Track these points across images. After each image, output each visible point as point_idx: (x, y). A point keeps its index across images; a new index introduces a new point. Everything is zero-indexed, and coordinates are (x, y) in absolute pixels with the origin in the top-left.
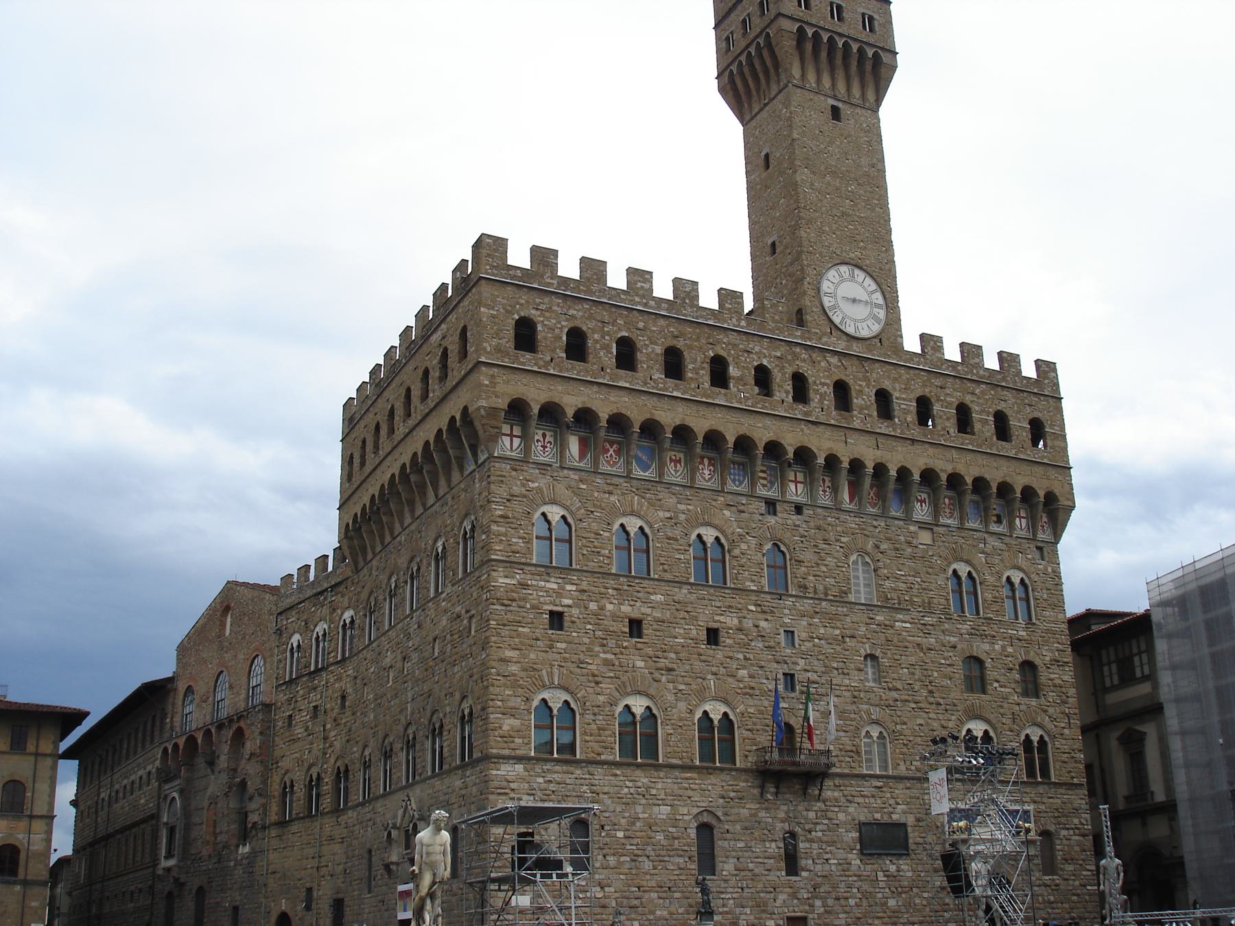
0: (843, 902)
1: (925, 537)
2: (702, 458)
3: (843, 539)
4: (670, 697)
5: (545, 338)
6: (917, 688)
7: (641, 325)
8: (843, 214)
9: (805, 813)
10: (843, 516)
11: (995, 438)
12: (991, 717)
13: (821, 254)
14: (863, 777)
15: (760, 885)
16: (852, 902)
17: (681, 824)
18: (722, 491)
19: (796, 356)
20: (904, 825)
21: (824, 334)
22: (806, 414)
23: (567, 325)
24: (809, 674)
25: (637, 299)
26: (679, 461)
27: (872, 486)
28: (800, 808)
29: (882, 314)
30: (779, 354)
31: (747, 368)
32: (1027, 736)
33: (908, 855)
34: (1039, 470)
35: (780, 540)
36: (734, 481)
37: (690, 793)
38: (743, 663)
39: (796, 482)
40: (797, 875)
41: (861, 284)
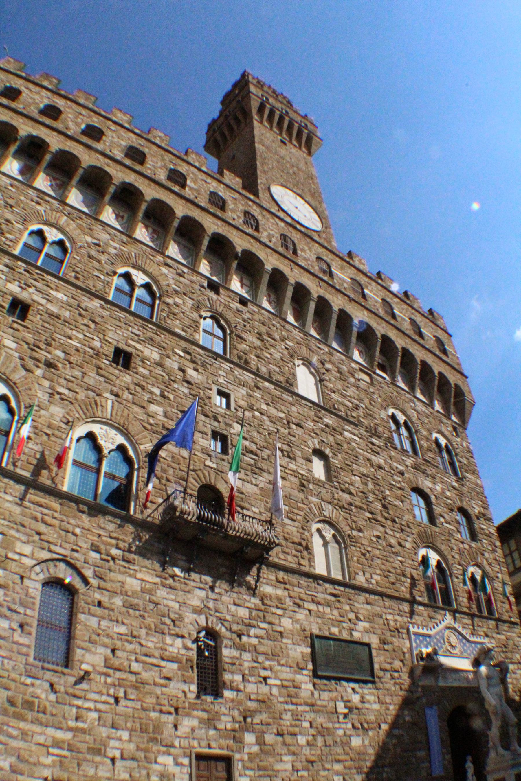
0: (289, 739)
4: (42, 396)
6: (371, 499)
9: (233, 608)
10: (288, 326)
12: (443, 548)
14: (316, 578)
15: (150, 700)
16: (302, 740)
17: (13, 566)
20: (368, 645)
24: (247, 443)
27: (314, 321)
28: (225, 598)
32: (472, 574)
33: (373, 682)
35: (221, 315)
37: (42, 528)
38: (158, 399)
40: (217, 694)
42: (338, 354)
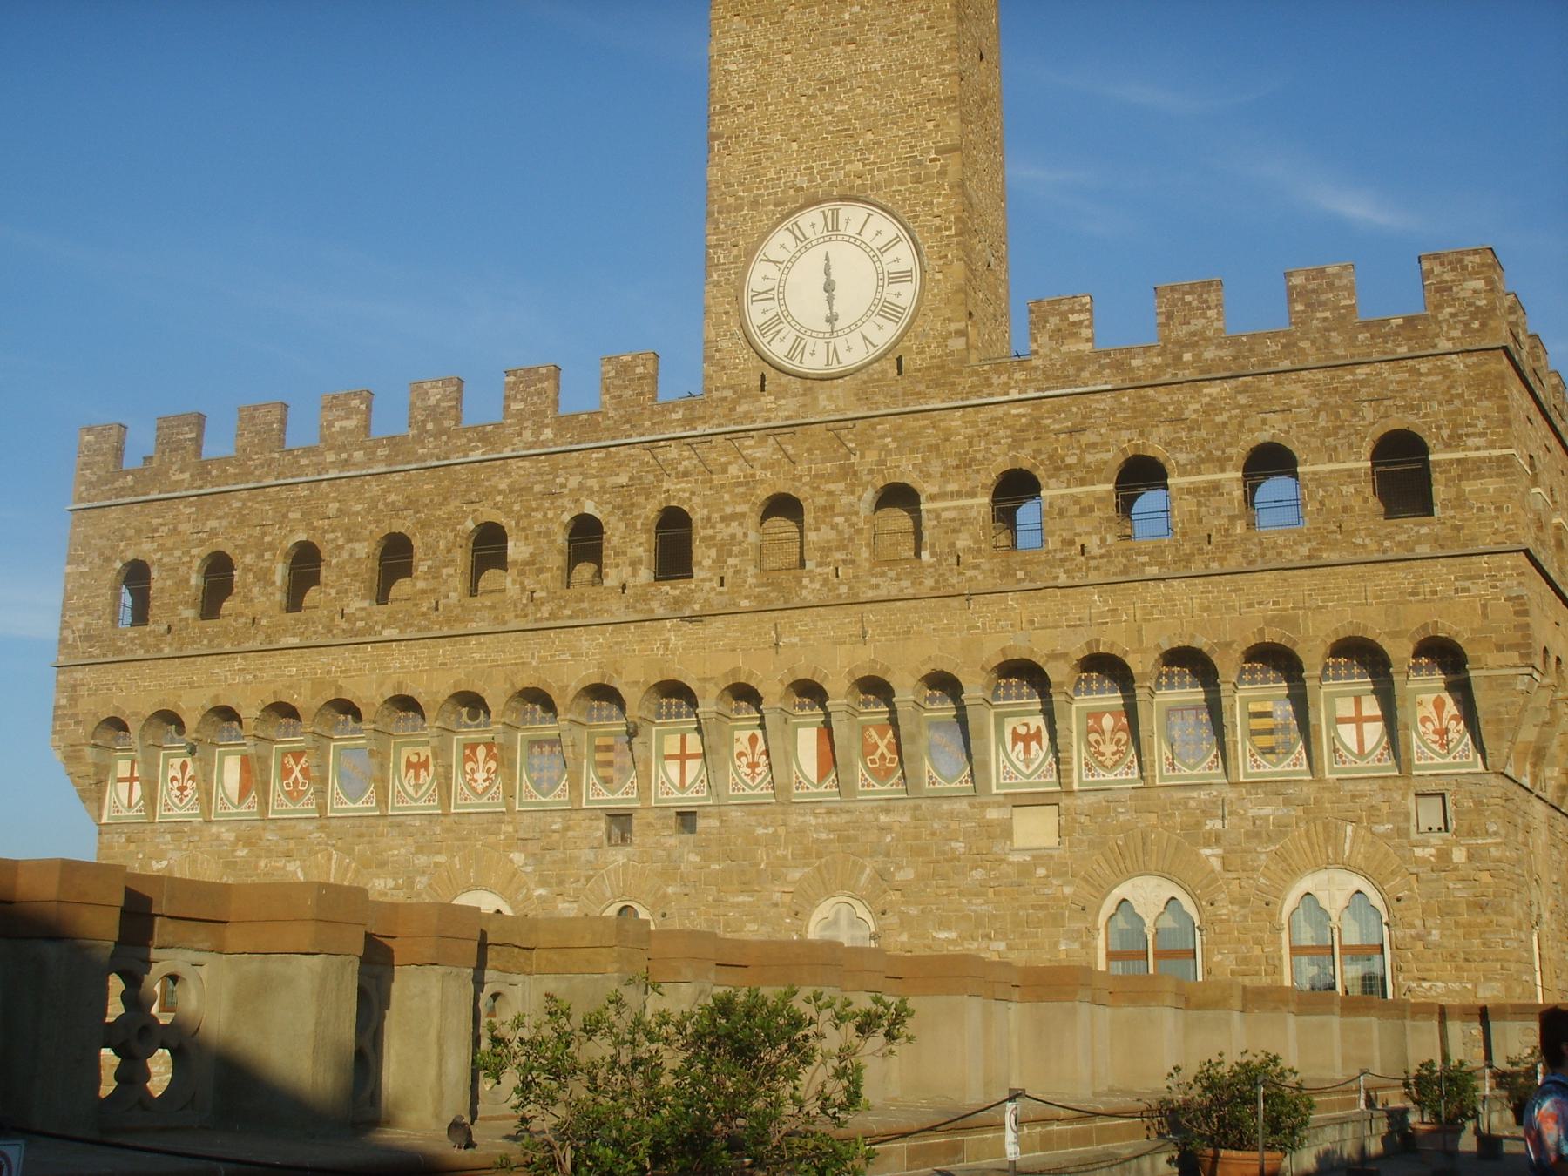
1: (1035, 831)
2: (473, 747)
3: (796, 875)
5: (162, 590)
7: (334, 506)
8: (826, 84)
10: (795, 820)
11: (1240, 528)
13: (754, 204)
18: (510, 810)
19: (663, 470)
21: (742, 394)
22: (677, 601)
23: (200, 553)
25: (330, 457)
26: (425, 765)
29: (906, 295)
30: (623, 479)
31: (547, 534)
34: (1402, 577)
36: (537, 784)
39: (683, 757)
41: (856, 241)
42: (946, 806)
